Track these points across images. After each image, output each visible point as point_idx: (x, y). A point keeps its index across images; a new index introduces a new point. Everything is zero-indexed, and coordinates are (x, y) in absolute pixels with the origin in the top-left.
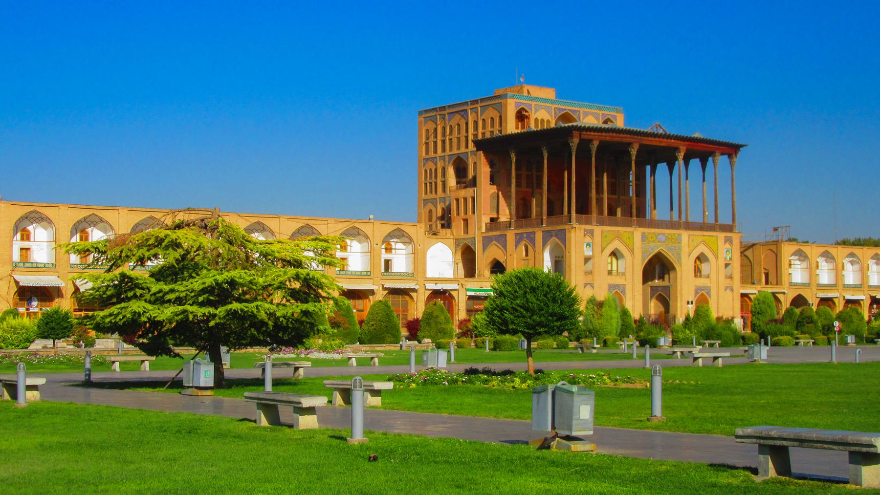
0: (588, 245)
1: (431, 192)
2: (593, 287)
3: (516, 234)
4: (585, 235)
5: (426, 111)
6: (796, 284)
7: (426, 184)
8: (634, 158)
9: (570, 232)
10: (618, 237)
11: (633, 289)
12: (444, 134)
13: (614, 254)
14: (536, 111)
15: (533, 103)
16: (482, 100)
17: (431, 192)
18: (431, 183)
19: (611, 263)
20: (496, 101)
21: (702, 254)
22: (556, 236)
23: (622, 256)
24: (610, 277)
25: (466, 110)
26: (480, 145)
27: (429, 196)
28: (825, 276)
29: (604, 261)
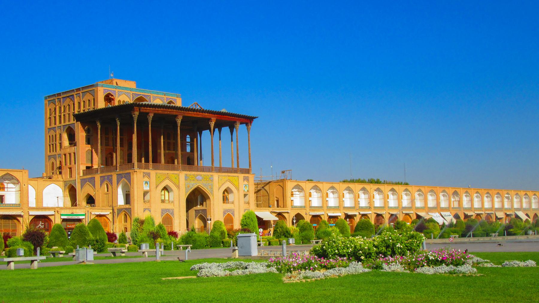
0: (146, 183)
1: (53, 151)
2: (150, 211)
3: (101, 177)
4: (144, 176)
5: (49, 97)
6: (296, 207)
7: (50, 145)
8: (179, 125)
9: (133, 174)
10: (168, 178)
11: (179, 212)
12: (60, 112)
13: (165, 188)
14: (119, 95)
15: (117, 90)
16: (83, 88)
17: (53, 151)
18: (53, 145)
19: (165, 195)
20: (91, 89)
21: (228, 187)
22: (125, 177)
23: (172, 190)
24: (163, 204)
25: (73, 95)
26: (79, 117)
27: (52, 153)
28: (315, 201)
29: (157, 194)
